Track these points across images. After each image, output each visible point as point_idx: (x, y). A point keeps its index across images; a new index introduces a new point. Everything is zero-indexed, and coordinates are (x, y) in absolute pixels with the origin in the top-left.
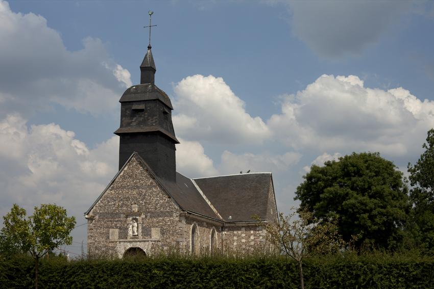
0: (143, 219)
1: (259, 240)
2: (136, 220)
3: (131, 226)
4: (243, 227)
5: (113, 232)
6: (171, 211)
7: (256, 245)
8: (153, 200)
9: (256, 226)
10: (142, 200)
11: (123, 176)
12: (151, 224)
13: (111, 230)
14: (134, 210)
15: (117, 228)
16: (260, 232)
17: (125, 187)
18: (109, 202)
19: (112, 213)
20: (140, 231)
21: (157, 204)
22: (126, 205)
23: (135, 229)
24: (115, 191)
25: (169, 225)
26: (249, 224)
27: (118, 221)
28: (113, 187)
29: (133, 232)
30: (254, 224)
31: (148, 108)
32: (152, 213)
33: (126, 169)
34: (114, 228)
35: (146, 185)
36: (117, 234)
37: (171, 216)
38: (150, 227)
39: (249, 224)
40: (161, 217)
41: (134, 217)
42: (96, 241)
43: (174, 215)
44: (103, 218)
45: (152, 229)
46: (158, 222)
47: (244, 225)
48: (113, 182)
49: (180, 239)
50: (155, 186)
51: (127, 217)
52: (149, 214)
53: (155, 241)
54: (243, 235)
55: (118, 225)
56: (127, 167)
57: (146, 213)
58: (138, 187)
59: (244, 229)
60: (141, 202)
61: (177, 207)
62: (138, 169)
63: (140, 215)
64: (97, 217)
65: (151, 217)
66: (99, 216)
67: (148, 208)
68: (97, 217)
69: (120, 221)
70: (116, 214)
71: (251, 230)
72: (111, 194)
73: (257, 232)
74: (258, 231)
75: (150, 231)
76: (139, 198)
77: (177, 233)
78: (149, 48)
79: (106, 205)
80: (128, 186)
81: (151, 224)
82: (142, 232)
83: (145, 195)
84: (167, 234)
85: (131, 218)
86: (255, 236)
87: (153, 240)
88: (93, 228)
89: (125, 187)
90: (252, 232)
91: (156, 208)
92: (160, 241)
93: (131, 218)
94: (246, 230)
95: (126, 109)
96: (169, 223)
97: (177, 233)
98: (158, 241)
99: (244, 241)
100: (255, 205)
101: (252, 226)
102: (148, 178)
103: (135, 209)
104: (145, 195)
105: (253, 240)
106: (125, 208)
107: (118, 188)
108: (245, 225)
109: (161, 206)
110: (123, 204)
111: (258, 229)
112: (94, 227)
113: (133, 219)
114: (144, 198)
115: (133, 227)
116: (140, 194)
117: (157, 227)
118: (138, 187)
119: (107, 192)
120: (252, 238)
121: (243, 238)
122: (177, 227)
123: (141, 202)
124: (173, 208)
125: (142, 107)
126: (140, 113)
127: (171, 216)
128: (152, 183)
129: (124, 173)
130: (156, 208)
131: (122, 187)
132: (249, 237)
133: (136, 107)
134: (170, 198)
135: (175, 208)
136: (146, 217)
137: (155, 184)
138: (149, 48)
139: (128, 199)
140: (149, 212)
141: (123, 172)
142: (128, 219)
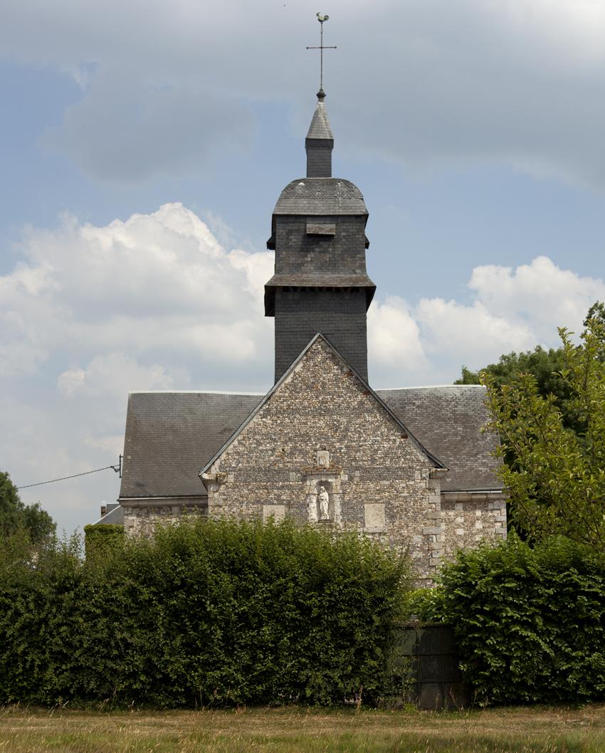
0: (342, 484)
2: (327, 486)
3: (314, 500)
4: (458, 502)
8: (365, 441)
9: (488, 501)
10: (340, 441)
11: (293, 384)
12: (363, 496)
14: (322, 463)
15: (280, 502)
16: (496, 513)
17: (297, 411)
18: (259, 443)
19: (268, 470)
20: (338, 510)
22: (301, 451)
23: (325, 505)
24: (275, 418)
25: (405, 497)
26: (474, 497)
27: (283, 487)
28: (268, 410)
29: (320, 513)
30: (485, 497)
31: (343, 234)
32: (366, 470)
33: (298, 368)
34: (273, 504)
35: (349, 408)
37: (410, 478)
38: (362, 503)
39: (474, 497)
41: (324, 479)
43: (417, 475)
44: (245, 481)
45: (366, 506)
46: (379, 492)
47: (462, 498)
48: (269, 398)
49: (432, 530)
50: (369, 411)
51: (304, 480)
52: (357, 473)
53: (373, 534)
54: (460, 520)
55: (284, 497)
56: (301, 365)
57: (351, 470)
58: (328, 411)
59: (460, 507)
60: (338, 445)
61: (422, 458)
62: (328, 371)
63: (336, 475)
64: (231, 478)
65: (362, 479)
66: (236, 477)
67: (355, 459)
68: (231, 478)
69: (290, 488)
70: (279, 472)
71: (475, 508)
72: (265, 425)
73: (490, 514)
74: (492, 510)
75: (362, 510)
76: (333, 436)
77: (425, 516)
78: (321, 96)
80: (305, 408)
81: (363, 496)
82: (343, 513)
83: (347, 430)
85: (315, 482)
86: (484, 521)
87: (370, 531)
88: (221, 502)
89: (297, 411)
90: (478, 513)
91: (373, 460)
92: (385, 534)
93: (315, 482)
94: (464, 509)
95: (290, 232)
96: (405, 494)
97: (425, 516)
98: (380, 534)
99: (460, 532)
100: (476, 455)
101: (480, 501)
102: (352, 391)
103: (325, 459)
104: (347, 430)
107: (279, 412)
108: (466, 498)
109: (386, 454)
110: (295, 448)
111: (490, 507)
112: (225, 500)
113: (321, 483)
114: (345, 437)
115: (318, 502)
116: (335, 427)
117: (377, 501)
118: (328, 411)
119: (255, 420)
120: (479, 525)
121: (459, 526)
122: (425, 503)
123: (338, 445)
124: (413, 461)
125: (327, 228)
126: (325, 245)
127: (410, 478)
128: (361, 403)
129: (294, 379)
130: (373, 460)
131: (291, 411)
132: (473, 524)
133: (312, 227)
134: (405, 437)
135: (419, 461)
136: (351, 479)
137: (368, 405)
138: (321, 96)
139: (305, 437)
140: (357, 468)
141: (292, 375)
142: (308, 483)
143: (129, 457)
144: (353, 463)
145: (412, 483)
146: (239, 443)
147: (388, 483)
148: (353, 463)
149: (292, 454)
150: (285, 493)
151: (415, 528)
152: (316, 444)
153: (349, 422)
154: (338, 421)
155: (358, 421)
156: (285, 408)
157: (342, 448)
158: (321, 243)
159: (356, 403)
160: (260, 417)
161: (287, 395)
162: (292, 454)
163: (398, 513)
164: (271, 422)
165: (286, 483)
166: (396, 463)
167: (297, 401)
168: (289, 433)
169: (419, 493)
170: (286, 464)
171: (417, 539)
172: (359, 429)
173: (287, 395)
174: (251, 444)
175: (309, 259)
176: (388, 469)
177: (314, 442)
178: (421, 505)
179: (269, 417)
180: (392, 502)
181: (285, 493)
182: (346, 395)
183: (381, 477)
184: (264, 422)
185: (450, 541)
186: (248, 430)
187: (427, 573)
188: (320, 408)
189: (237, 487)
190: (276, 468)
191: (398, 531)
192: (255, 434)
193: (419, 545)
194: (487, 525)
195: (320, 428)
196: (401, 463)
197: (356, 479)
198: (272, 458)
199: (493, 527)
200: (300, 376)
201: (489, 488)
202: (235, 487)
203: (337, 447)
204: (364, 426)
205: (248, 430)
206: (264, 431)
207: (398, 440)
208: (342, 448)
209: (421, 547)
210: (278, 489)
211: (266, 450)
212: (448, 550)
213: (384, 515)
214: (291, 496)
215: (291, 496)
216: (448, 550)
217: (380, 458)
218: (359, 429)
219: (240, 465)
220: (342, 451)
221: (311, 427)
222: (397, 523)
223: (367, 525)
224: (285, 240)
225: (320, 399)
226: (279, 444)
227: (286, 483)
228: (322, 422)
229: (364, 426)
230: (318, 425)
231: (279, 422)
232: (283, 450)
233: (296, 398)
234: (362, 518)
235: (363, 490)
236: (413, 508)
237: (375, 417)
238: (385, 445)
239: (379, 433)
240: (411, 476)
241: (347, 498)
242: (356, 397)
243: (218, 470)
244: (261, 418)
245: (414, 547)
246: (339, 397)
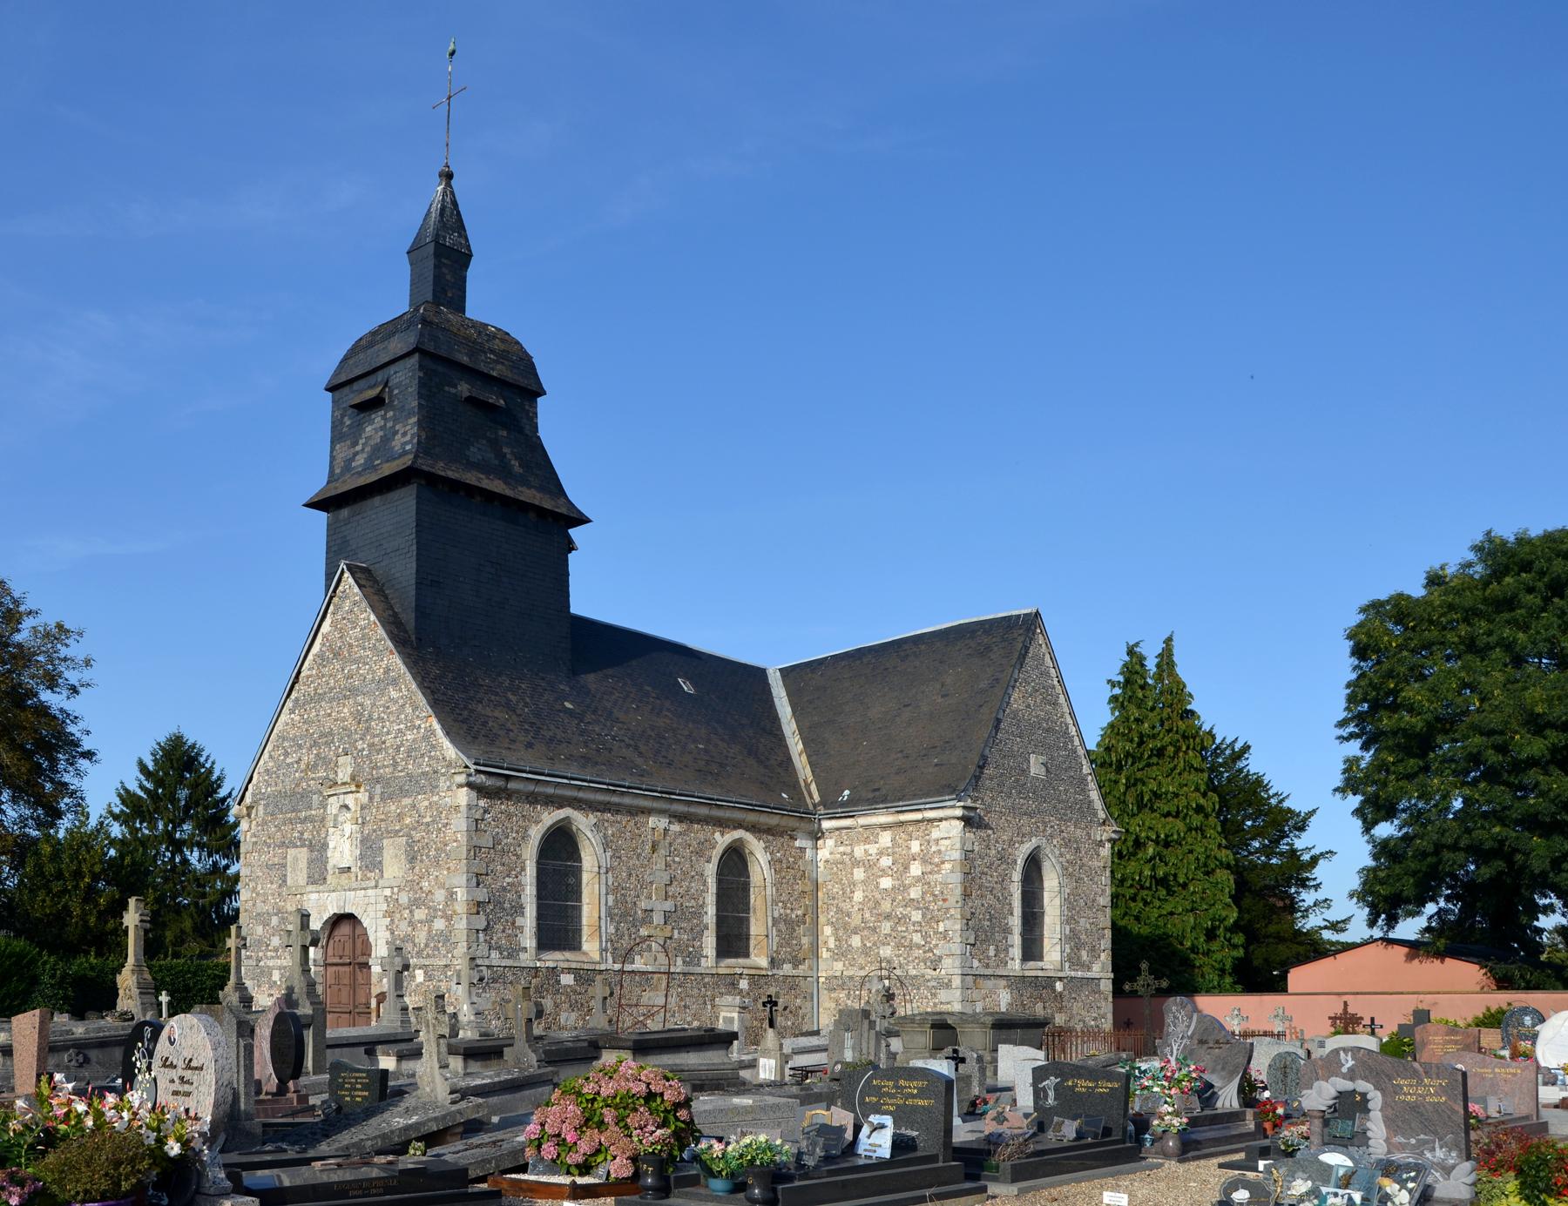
1: (939, 877)
5: (296, 859)
6: (435, 772)
7: (929, 898)
13: (292, 852)
25: (428, 824)
28: (297, 699)
32: (387, 784)
34: (297, 847)
35: (373, 680)
36: (303, 864)
46: (400, 817)
75: (381, 849)
84: (422, 861)
86: (924, 861)
89: (321, 697)
91: (395, 764)
96: (428, 819)
105: (918, 879)
120: (916, 869)
121: (884, 872)
127: (434, 788)
132: (906, 868)
138: (448, 176)
153: (373, 705)
159: (382, 670)
183: (404, 793)
185: (870, 900)
194: (929, 868)
197: (377, 798)
199: (939, 872)
201: (923, 800)
204: (388, 708)
209: (443, 911)
212: (867, 915)
213: (403, 857)
216: (867, 915)
228: (346, 710)
236: (435, 843)
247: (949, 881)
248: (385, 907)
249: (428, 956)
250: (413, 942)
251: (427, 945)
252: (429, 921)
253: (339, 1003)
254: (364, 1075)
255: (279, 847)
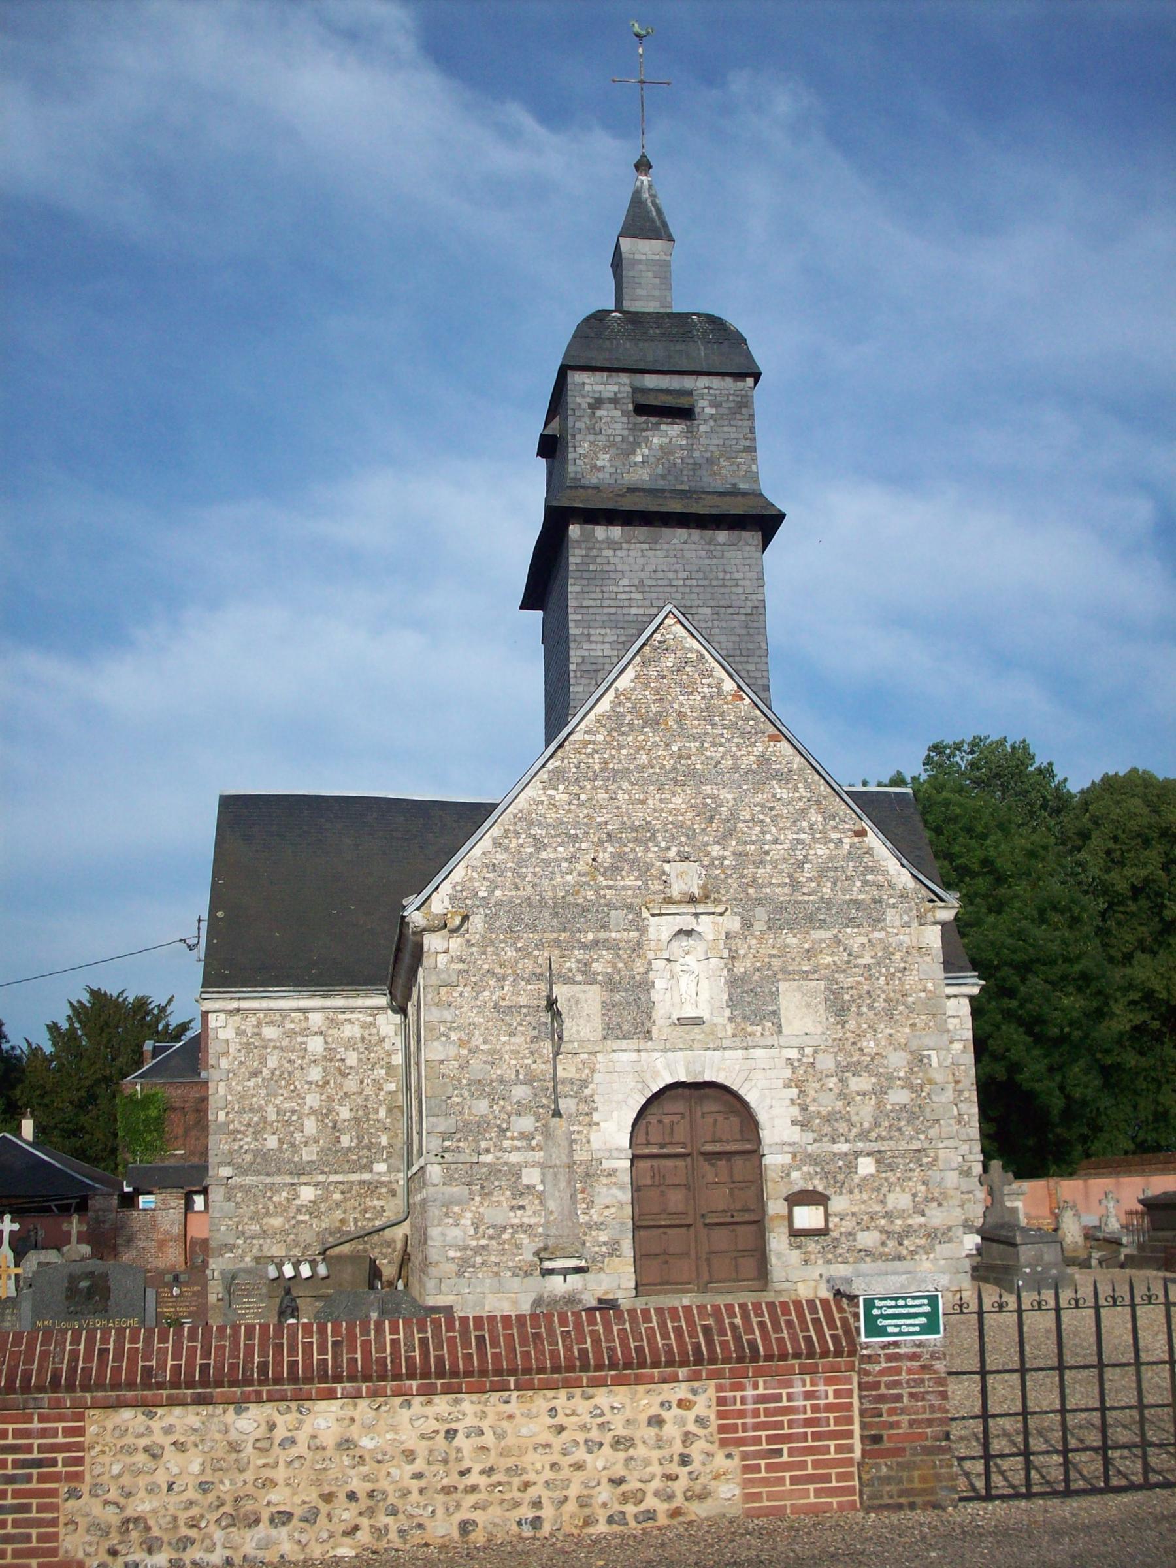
6: (875, 901)
8: (776, 841)
10: (721, 840)
21: (800, 865)
24: (575, 789)
25: (867, 967)
27: (596, 943)
32: (781, 908)
34: (576, 983)
35: (735, 768)
38: (774, 979)
40: (822, 925)
42: (473, 1051)
45: (782, 986)
52: (761, 913)
56: (630, 673)
57: (746, 908)
58: (692, 774)
60: (715, 850)
64: (477, 922)
65: (771, 926)
66: (489, 919)
69: (612, 946)
70: (584, 910)
72: (553, 805)
75: (774, 995)
79: (522, 863)
80: (641, 769)
81: (776, 963)
83: (734, 816)
84: (859, 1014)
91: (795, 885)
96: (867, 960)
106: (631, 881)
107: (585, 776)
109: (822, 872)
110: (619, 856)
114: (731, 832)
122: (910, 980)
123: (715, 850)
129: (616, 703)
130: (795, 885)
136: (747, 925)
139: (644, 833)
140: (760, 902)
141: (611, 695)
143: (220, 914)
144: (751, 891)
145: (882, 935)
146: (496, 844)
147: (829, 934)
148: (751, 891)
149: (614, 869)
150: (601, 956)
151: (891, 1035)
152: (669, 849)
153: (738, 800)
154: (714, 797)
155: (759, 798)
156: (597, 767)
157: (724, 858)
158: (663, 427)
159: (752, 758)
160: (541, 786)
161: (600, 738)
162: (614, 869)
163: (854, 1001)
164: (566, 797)
165: (603, 935)
166: (844, 891)
167: (624, 752)
168: (606, 823)
169: (897, 957)
170: (602, 893)
171: (897, 1061)
172: (761, 817)
173: (600, 738)
174: (521, 846)
175: (639, 459)
176: (829, 904)
177: (663, 844)
178: (902, 985)
179: (561, 787)
180: (840, 977)
181: (601, 956)
182: (729, 740)
183: (812, 921)
184: (552, 797)
186: (515, 816)
187: (922, 1137)
188: (674, 768)
189: (492, 943)
190: (580, 901)
191: (854, 1043)
192: (531, 823)
193: (902, 1074)
195: (676, 812)
196: (856, 891)
197: (759, 927)
198: (569, 878)
200: (628, 699)
202: (486, 943)
203: (714, 854)
204: (771, 809)
205: (515, 816)
206: (551, 817)
207: (846, 840)
208: (724, 858)
210: (584, 947)
211: (556, 860)
213: (822, 1007)
214: (614, 966)
215: (614, 966)
217: (811, 880)
218: (761, 817)
219: (498, 893)
220: (726, 863)
221: (655, 810)
222: (851, 1025)
223: (786, 1030)
224: (587, 420)
225: (675, 748)
226: (584, 846)
227: (603, 935)
229: (771, 809)
230: (671, 806)
231: (583, 797)
232: (594, 860)
233: (622, 747)
234: (774, 1012)
235: (774, 952)
237: (796, 790)
238: (820, 852)
239: (805, 824)
240: (879, 921)
241: (739, 969)
242: (753, 745)
243: (447, 903)
244: (544, 788)
245: (890, 1078)
246: (714, 744)
247: (961, 1061)
248: (788, 1073)
249: (879, 1138)
250: (849, 1120)
251: (877, 1124)
252: (880, 1092)
253: (664, 1211)
254: (926, 1301)
255: (528, 982)
